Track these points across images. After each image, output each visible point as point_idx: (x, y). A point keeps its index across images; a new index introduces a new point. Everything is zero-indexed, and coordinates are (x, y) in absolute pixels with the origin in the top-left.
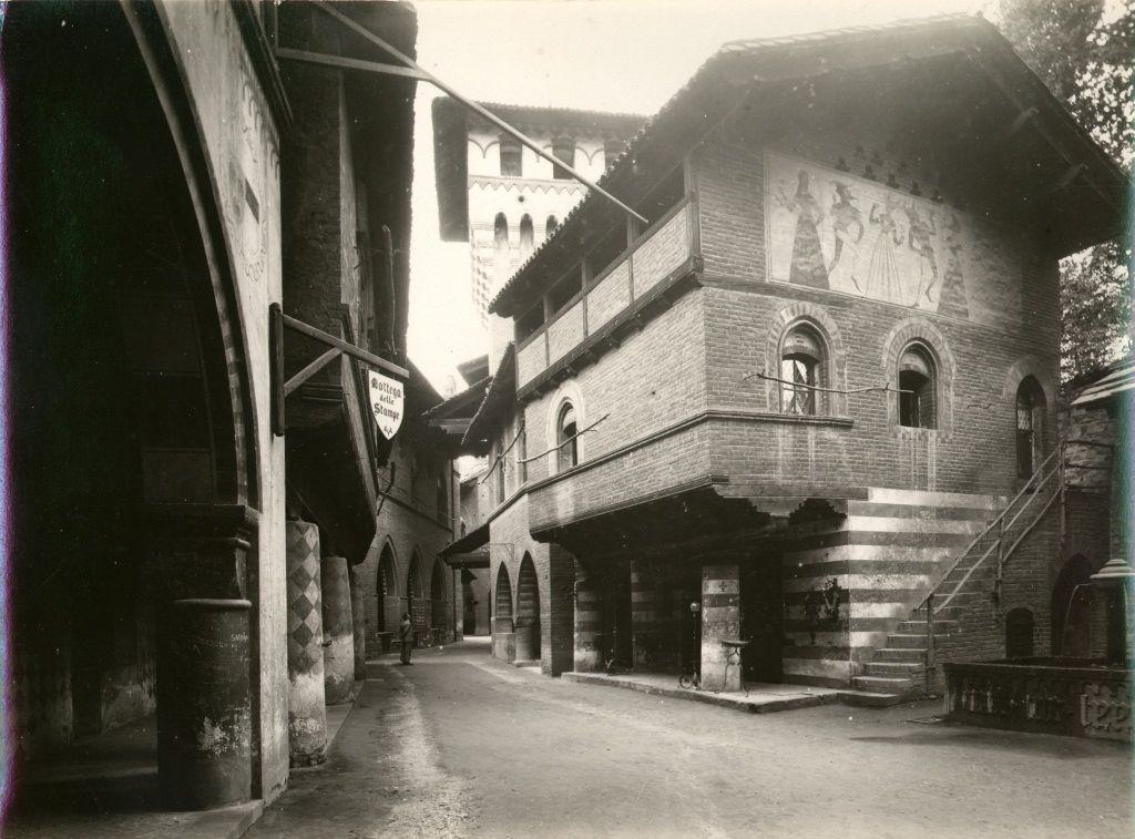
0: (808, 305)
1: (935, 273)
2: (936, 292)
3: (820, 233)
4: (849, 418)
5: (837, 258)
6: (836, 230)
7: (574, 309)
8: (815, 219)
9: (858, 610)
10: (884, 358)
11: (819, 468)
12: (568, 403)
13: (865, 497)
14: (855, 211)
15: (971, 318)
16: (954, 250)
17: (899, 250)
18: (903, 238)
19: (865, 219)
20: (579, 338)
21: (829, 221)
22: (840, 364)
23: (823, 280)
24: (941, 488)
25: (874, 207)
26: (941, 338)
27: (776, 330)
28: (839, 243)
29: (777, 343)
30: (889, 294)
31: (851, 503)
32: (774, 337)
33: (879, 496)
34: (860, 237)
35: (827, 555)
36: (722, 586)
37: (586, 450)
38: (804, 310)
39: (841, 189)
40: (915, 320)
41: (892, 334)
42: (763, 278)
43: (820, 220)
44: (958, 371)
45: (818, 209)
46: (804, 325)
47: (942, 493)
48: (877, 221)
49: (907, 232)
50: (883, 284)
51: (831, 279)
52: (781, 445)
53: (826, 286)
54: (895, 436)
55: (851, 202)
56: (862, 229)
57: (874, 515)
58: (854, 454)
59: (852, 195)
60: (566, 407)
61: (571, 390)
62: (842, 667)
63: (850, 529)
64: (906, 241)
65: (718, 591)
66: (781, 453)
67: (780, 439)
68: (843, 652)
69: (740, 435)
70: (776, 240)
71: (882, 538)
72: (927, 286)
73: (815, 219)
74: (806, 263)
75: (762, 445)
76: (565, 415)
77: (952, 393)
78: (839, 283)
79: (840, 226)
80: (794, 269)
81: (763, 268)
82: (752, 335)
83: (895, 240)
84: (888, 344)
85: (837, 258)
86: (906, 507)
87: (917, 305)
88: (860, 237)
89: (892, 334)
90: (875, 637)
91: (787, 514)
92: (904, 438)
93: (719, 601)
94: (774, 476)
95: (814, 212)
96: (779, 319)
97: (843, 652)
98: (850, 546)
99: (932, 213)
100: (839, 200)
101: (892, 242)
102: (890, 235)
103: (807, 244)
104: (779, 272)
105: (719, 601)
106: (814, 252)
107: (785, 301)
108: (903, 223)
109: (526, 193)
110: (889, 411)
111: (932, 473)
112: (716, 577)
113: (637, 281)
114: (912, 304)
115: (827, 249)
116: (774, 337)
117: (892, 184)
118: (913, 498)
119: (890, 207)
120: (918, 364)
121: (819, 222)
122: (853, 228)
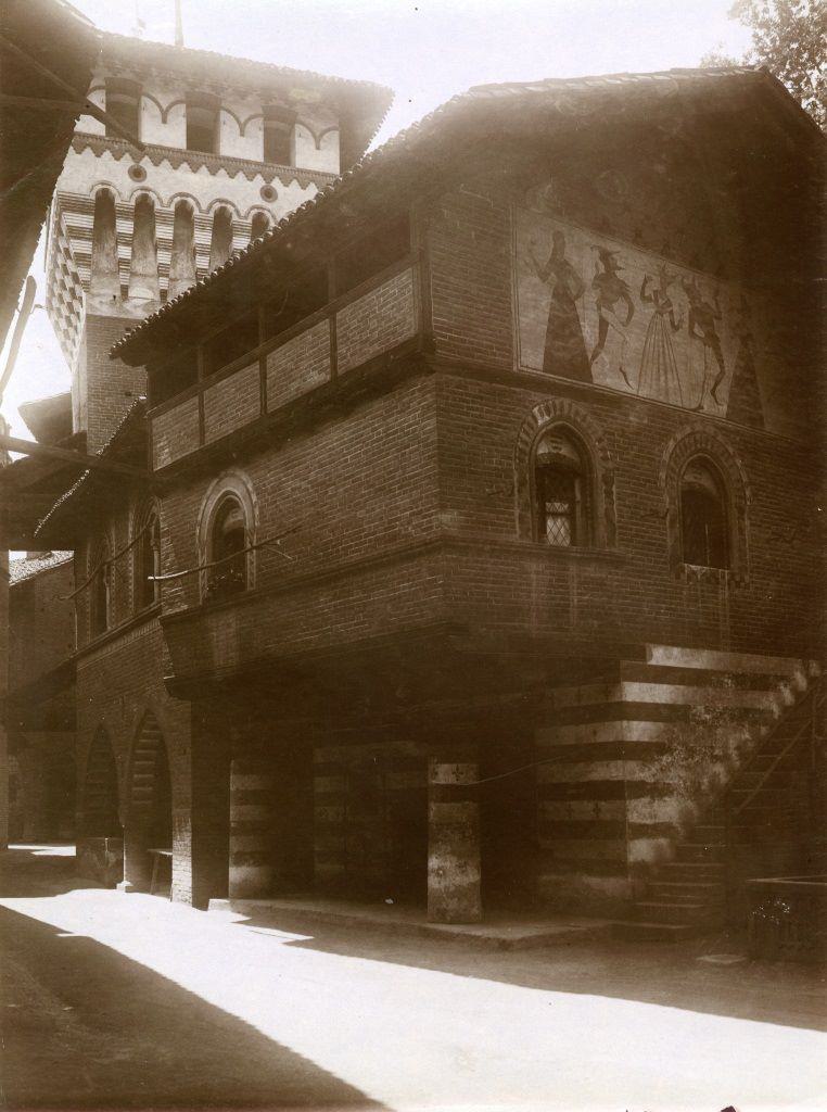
0: (567, 401)
1: (722, 367)
2: (724, 391)
3: (580, 311)
5: (601, 345)
6: (599, 309)
7: (247, 370)
8: (574, 293)
9: (639, 811)
10: (663, 475)
12: (231, 500)
13: (643, 655)
14: (623, 284)
15: (768, 428)
16: (746, 339)
17: (679, 338)
18: (681, 321)
19: (635, 296)
20: (253, 410)
21: (591, 297)
23: (581, 367)
25: (646, 281)
26: (731, 450)
27: (528, 434)
28: (603, 324)
29: (528, 449)
30: (667, 393)
31: (624, 663)
32: (526, 444)
33: (660, 656)
34: (629, 318)
35: (595, 733)
36: (457, 773)
37: (259, 569)
38: (562, 409)
39: (605, 256)
40: (698, 427)
41: (671, 444)
42: (511, 364)
43: (581, 291)
44: (754, 495)
45: (577, 279)
46: (563, 428)
47: (738, 655)
48: (649, 299)
49: (687, 314)
50: (659, 379)
51: (595, 369)
52: (534, 584)
53: (589, 378)
54: (678, 577)
55: (618, 273)
56: (631, 310)
58: (626, 598)
59: (619, 264)
60: (228, 505)
61: (238, 484)
63: (623, 699)
64: (686, 326)
65: (452, 780)
66: (534, 595)
67: (534, 576)
68: (619, 867)
69: (481, 569)
70: (526, 317)
71: (665, 712)
72: (712, 383)
73: (574, 293)
74: (564, 348)
75: (509, 584)
76: (225, 517)
77: (747, 522)
78: (606, 377)
79: (605, 302)
80: (548, 356)
81: (509, 351)
82: (497, 438)
83: (672, 323)
84: (666, 457)
85: (601, 345)
87: (701, 407)
88: (629, 318)
89: (671, 444)
90: (658, 849)
92: (689, 578)
94: (526, 625)
95: (571, 283)
96: (530, 418)
99: (717, 293)
100: (602, 269)
101: (668, 326)
102: (666, 317)
103: (563, 327)
104: (531, 359)
106: (573, 335)
107: (536, 396)
108: (680, 302)
109: (146, 163)
110: (669, 542)
113: (342, 350)
114: (694, 406)
115: (589, 333)
116: (526, 444)
117: (665, 252)
118: (700, 660)
119: (666, 281)
121: (578, 297)
122: (620, 308)
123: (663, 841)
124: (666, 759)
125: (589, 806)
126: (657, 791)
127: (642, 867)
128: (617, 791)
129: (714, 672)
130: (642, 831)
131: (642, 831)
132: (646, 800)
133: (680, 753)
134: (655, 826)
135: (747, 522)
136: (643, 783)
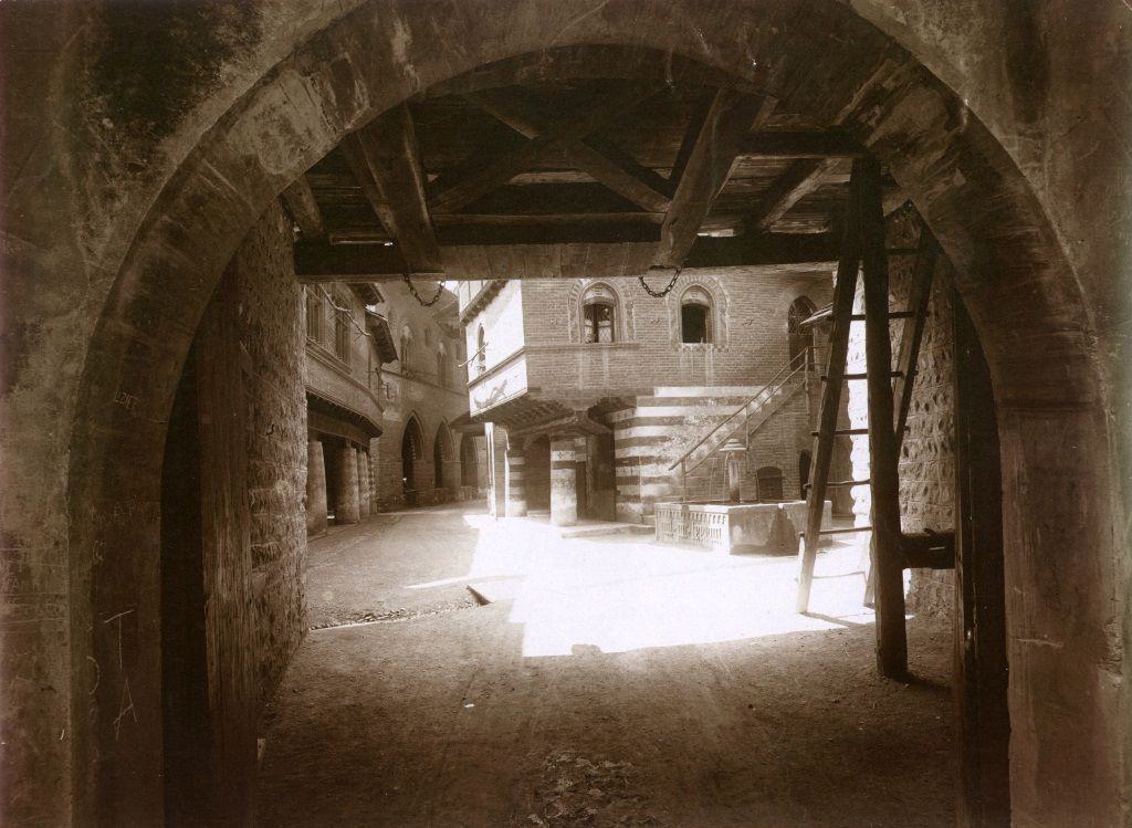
4: (637, 342)
9: (646, 471)
11: (612, 377)
13: (652, 393)
22: (629, 306)
24: (719, 384)
31: (639, 398)
33: (663, 392)
54: (677, 350)
57: (659, 405)
62: (636, 507)
77: (727, 316)
86: (687, 398)
91: (587, 408)
93: (562, 465)
97: (637, 498)
98: (639, 428)
105: (562, 465)
111: (710, 373)
112: (556, 449)
118: (694, 392)
120: (700, 298)
123: (665, 485)
124: (667, 444)
125: (629, 468)
126: (660, 460)
127: (650, 499)
128: (634, 461)
129: (702, 398)
130: (650, 480)
131: (650, 480)
132: (654, 465)
133: (676, 440)
134: (659, 478)
135: (727, 316)
136: (652, 457)
